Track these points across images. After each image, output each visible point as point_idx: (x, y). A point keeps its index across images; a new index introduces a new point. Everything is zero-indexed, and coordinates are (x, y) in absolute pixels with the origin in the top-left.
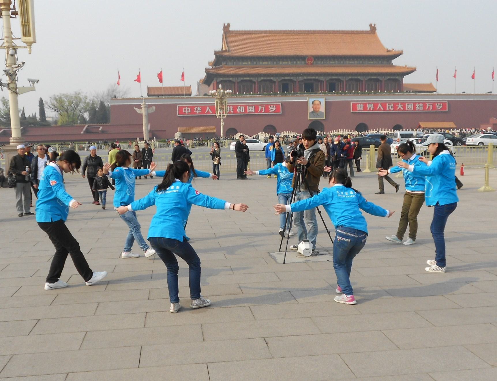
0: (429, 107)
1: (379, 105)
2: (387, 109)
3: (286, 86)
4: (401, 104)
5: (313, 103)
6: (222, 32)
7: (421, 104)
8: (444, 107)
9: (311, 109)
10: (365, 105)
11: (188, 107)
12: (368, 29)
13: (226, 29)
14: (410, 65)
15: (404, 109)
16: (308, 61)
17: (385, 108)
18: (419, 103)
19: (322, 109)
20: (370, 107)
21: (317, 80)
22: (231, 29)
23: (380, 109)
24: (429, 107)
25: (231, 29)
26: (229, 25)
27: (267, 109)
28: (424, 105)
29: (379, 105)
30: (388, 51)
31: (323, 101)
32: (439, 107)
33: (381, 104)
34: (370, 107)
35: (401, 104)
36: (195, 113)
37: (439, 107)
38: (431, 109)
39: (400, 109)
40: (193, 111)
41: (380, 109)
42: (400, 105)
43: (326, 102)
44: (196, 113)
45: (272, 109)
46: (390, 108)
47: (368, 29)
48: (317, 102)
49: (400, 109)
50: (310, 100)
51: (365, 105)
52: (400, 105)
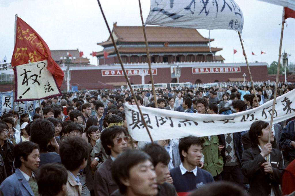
0: (231, 70)
2: (211, 71)
4: (218, 68)
7: (227, 69)
8: (238, 70)
11: (108, 71)
14: (219, 47)
15: (219, 71)
16: (165, 44)
21: (171, 56)
22: (118, 25)
24: (231, 70)
25: (118, 25)
26: (116, 23)
30: (206, 39)
32: (236, 69)
36: (112, 75)
39: (217, 71)
40: (110, 74)
42: (217, 70)
44: (112, 75)
46: (212, 71)
49: (217, 71)
52: (217, 70)
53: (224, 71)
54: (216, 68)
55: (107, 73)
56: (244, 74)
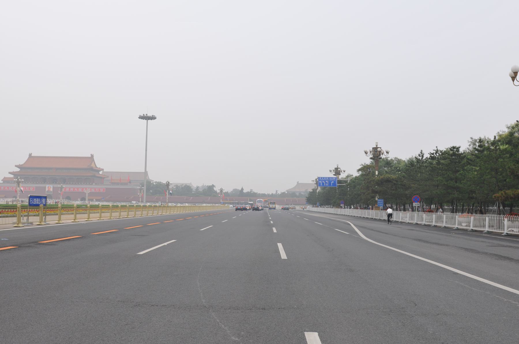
3: (44, 181)
6: (28, 157)
9: (47, 190)
10: (70, 189)
12: (90, 156)
13: (30, 155)
19: (51, 190)
20: (72, 189)
27: (29, 189)
28: (95, 190)
31: (52, 186)
34: (72, 189)
43: (53, 187)
45: (31, 189)
47: (90, 156)
50: (47, 186)
51: (70, 189)
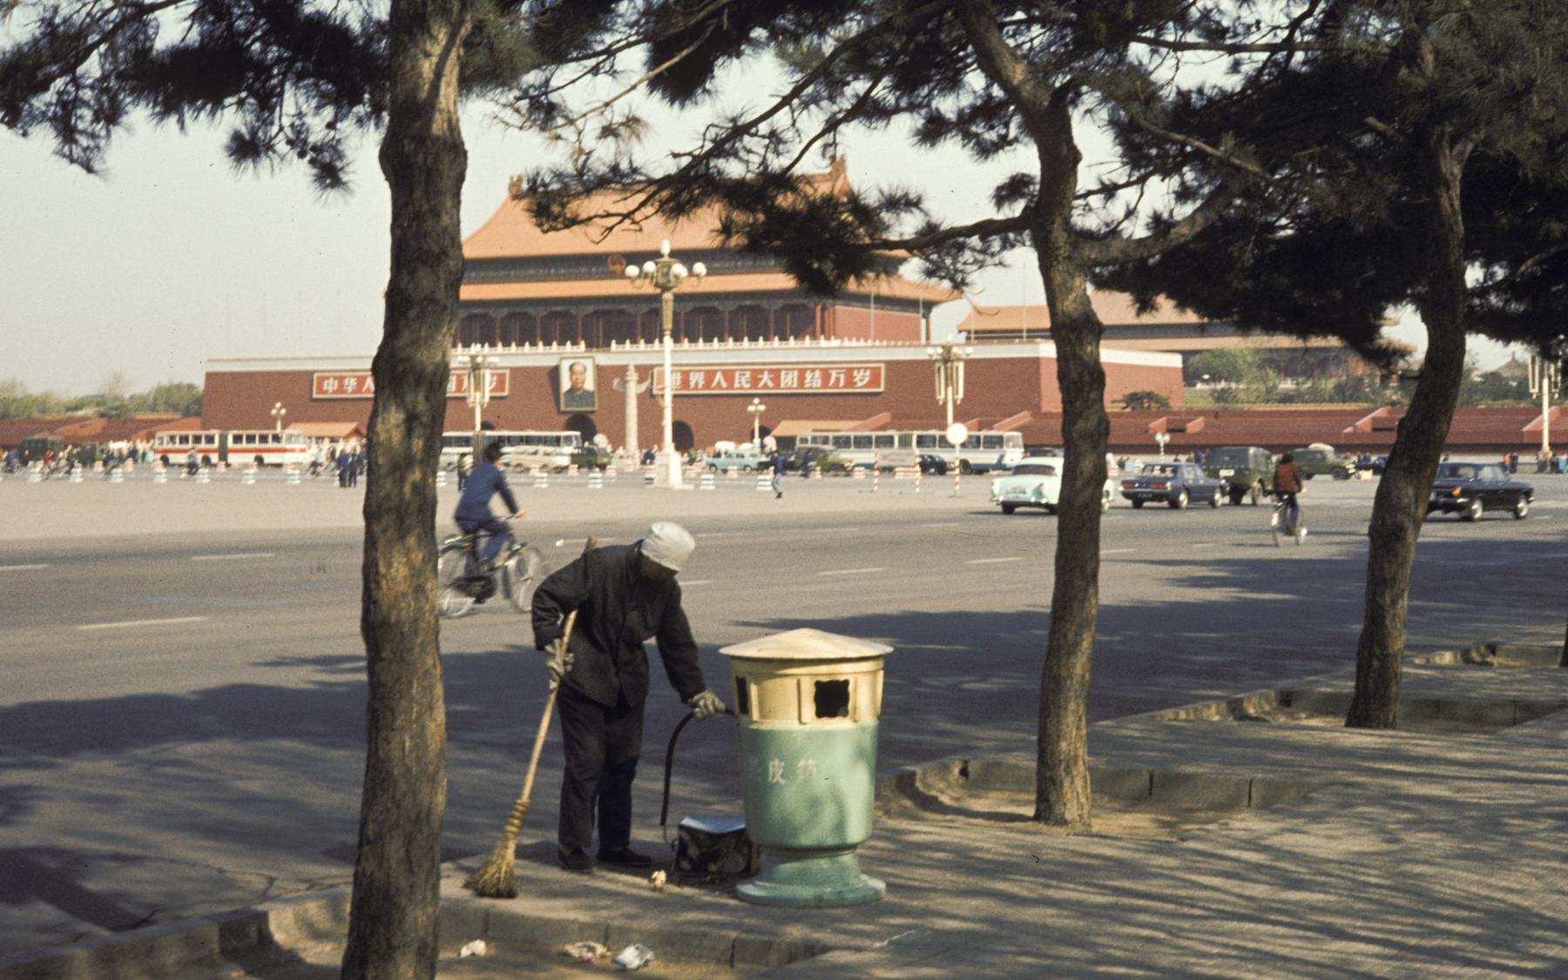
0: (838, 380)
1: (719, 376)
2: (737, 385)
4: (771, 371)
5: (571, 367)
7: (817, 373)
8: (874, 381)
9: (566, 385)
15: (777, 385)
17: (731, 385)
18: (813, 370)
19: (589, 385)
20: (697, 379)
23: (719, 386)
24: (838, 380)
28: (826, 375)
29: (719, 376)
31: (589, 364)
32: (862, 380)
33: (724, 372)
35: (771, 371)
37: (862, 380)
38: (842, 383)
39: (765, 386)
40: (341, 389)
41: (719, 386)
42: (766, 378)
48: (578, 368)
49: (765, 386)
52: (766, 378)
53: (801, 385)
54: (762, 371)
55: (330, 386)
56: (278, 405)
